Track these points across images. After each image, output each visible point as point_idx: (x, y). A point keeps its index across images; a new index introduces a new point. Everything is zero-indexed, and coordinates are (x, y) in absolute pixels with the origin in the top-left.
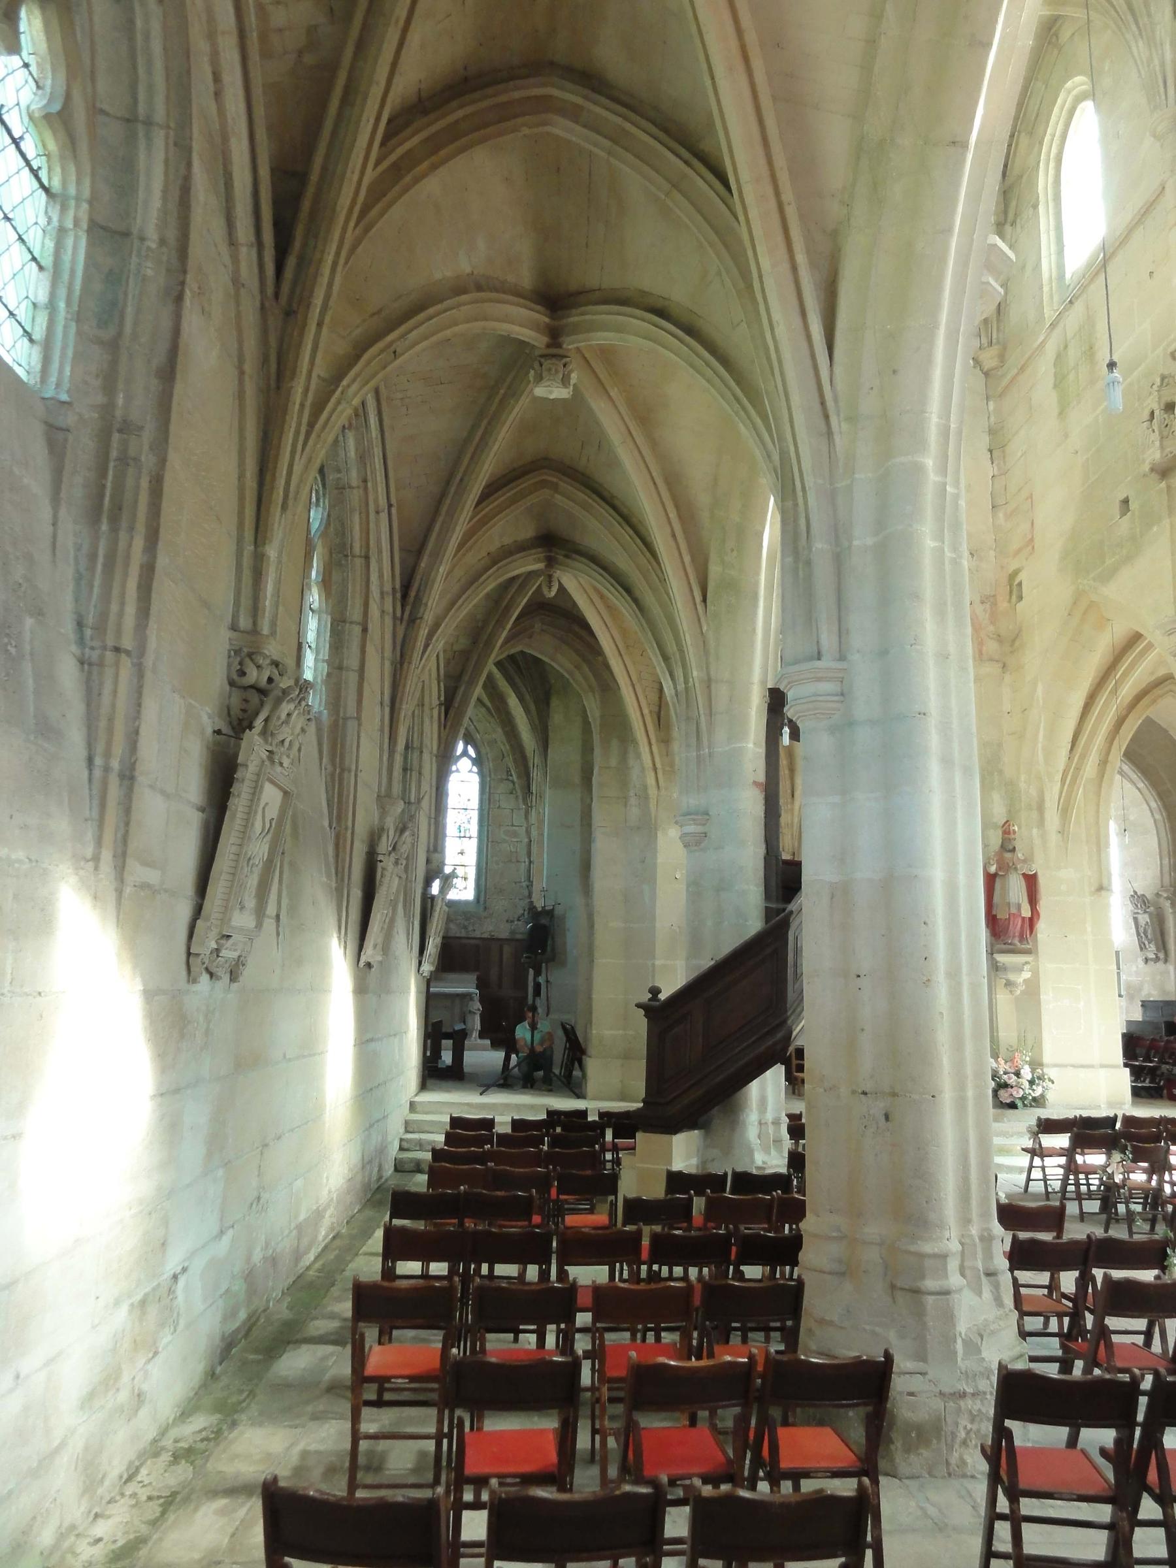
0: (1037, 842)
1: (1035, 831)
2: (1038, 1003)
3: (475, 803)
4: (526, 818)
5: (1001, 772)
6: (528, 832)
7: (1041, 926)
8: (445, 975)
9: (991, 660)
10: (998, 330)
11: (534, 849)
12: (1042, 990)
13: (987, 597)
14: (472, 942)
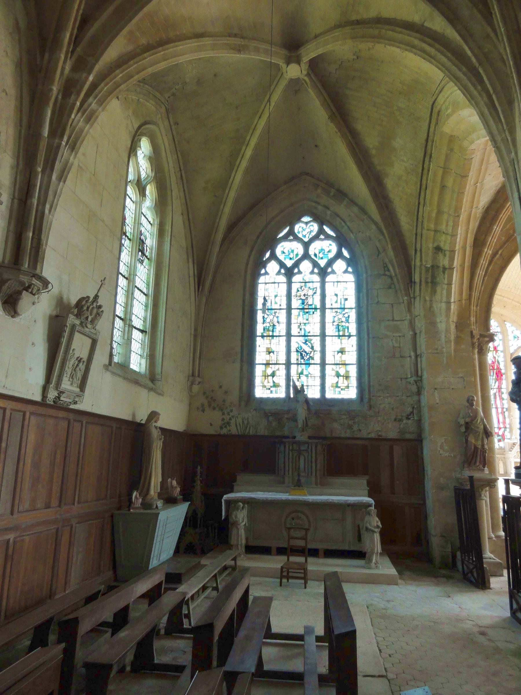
3: (352, 302)
4: (409, 310)
6: (412, 325)
11: (422, 341)
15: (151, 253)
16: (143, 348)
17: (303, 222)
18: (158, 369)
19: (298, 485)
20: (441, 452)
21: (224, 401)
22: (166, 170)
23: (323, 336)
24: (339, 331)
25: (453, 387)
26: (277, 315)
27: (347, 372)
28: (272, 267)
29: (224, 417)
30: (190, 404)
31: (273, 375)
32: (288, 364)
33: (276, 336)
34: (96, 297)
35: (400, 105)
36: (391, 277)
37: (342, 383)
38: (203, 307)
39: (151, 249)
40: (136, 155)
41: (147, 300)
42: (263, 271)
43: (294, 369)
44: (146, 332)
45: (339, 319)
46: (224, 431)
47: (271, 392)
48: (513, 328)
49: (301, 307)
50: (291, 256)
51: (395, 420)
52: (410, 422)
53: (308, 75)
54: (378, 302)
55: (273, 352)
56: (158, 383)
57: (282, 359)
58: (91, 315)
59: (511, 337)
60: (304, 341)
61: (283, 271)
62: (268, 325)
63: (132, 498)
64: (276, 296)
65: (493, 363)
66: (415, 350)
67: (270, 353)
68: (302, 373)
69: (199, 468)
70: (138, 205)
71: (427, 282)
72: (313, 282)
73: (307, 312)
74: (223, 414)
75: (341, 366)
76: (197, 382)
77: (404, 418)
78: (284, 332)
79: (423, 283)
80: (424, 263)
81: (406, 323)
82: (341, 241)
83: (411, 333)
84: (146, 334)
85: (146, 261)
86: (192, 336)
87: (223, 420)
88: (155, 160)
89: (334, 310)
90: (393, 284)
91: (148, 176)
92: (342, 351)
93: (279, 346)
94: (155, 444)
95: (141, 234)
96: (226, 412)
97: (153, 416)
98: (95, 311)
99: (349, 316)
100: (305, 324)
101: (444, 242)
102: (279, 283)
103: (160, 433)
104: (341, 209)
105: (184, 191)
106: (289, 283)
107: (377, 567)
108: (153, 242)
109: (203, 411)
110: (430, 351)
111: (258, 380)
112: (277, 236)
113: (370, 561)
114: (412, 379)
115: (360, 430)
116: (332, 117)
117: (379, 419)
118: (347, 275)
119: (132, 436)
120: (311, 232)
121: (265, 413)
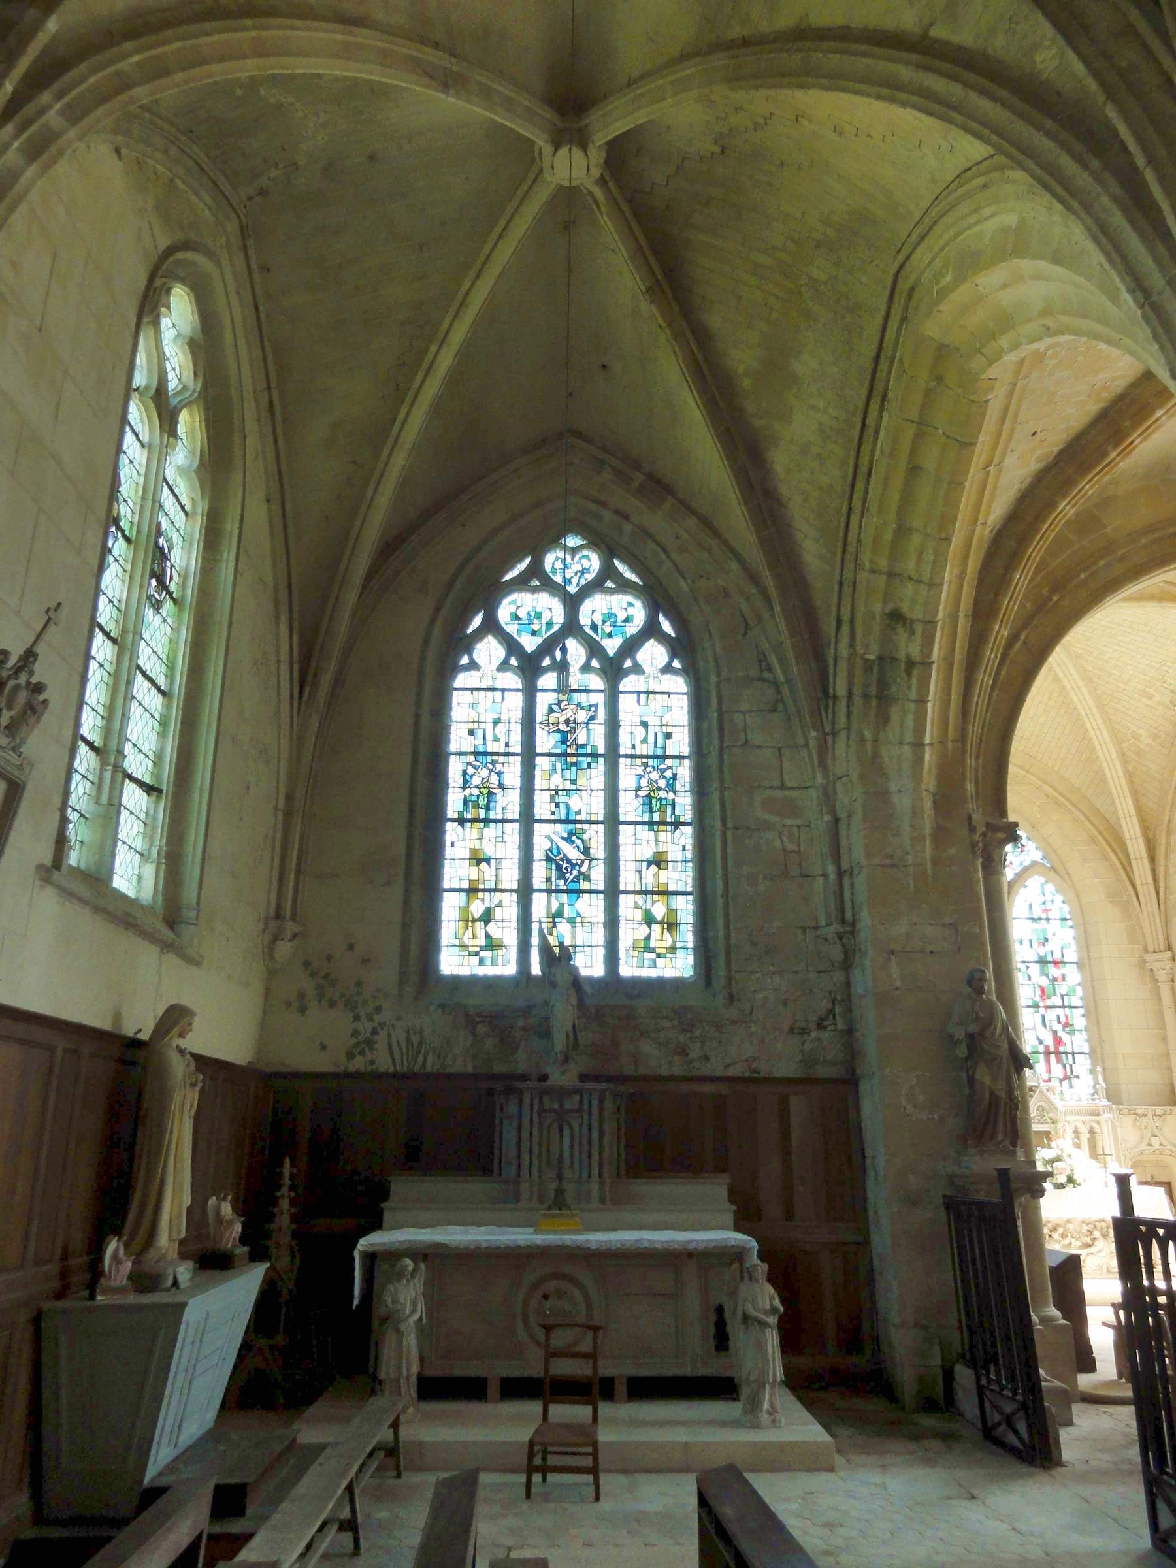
3: (681, 743)
4: (823, 764)
6: (828, 798)
8: (642, 1187)
14: (707, 1088)
15: (183, 586)
16: (148, 834)
17: (565, 548)
18: (190, 893)
19: (559, 1202)
20: (910, 1109)
21: (359, 984)
22: (233, 380)
23: (612, 822)
24: (651, 811)
25: (930, 948)
26: (499, 767)
27: (671, 911)
28: (489, 651)
29: (357, 1025)
30: (267, 993)
31: (487, 917)
32: (525, 892)
33: (496, 821)
34: (29, 656)
35: (815, 273)
36: (776, 685)
37: (660, 938)
38: (310, 741)
39: (184, 577)
40: (156, 323)
41: (168, 706)
42: (465, 660)
43: (539, 903)
44: (160, 791)
45: (651, 782)
46: (358, 1064)
47: (482, 962)
49: (559, 751)
50: (536, 627)
51: (792, 1030)
52: (826, 1035)
53: (602, 182)
54: (746, 742)
55: (488, 861)
56: (187, 931)
57: (511, 877)
58: (10, 707)
60: (565, 835)
61: (514, 661)
62: (476, 792)
63: (101, 1259)
64: (496, 722)
66: (836, 856)
67: (478, 862)
68: (559, 914)
69: (287, 1162)
70: (158, 453)
71: (866, 696)
72: (587, 691)
73: (574, 764)
74: (357, 1018)
75: (656, 897)
76: (289, 934)
77: (813, 1026)
78: (514, 812)
79: (858, 700)
80: (860, 650)
81: (813, 793)
82: (657, 597)
83: (827, 818)
84: (159, 798)
85: (169, 603)
86: (280, 816)
87: (356, 1033)
88: (205, 346)
89: (639, 761)
90: (782, 701)
91: (185, 388)
92: (659, 861)
93: (503, 844)
94: (177, 1098)
95: (159, 533)
96: (363, 1014)
97: (175, 1018)
98: (23, 696)
99: (675, 777)
100: (568, 792)
101: (909, 599)
102: (503, 690)
103: (193, 1067)
104: (657, 521)
105: (276, 441)
106: (530, 693)
107: (774, 1421)
108: (189, 559)
109: (303, 1010)
110: (877, 861)
111: (448, 931)
112: (503, 577)
113: (754, 1404)
114: (831, 930)
115: (707, 1058)
116: (654, 291)
117: (753, 1029)
118: (668, 677)
119: (116, 1077)
120: (584, 571)
121: (467, 1015)
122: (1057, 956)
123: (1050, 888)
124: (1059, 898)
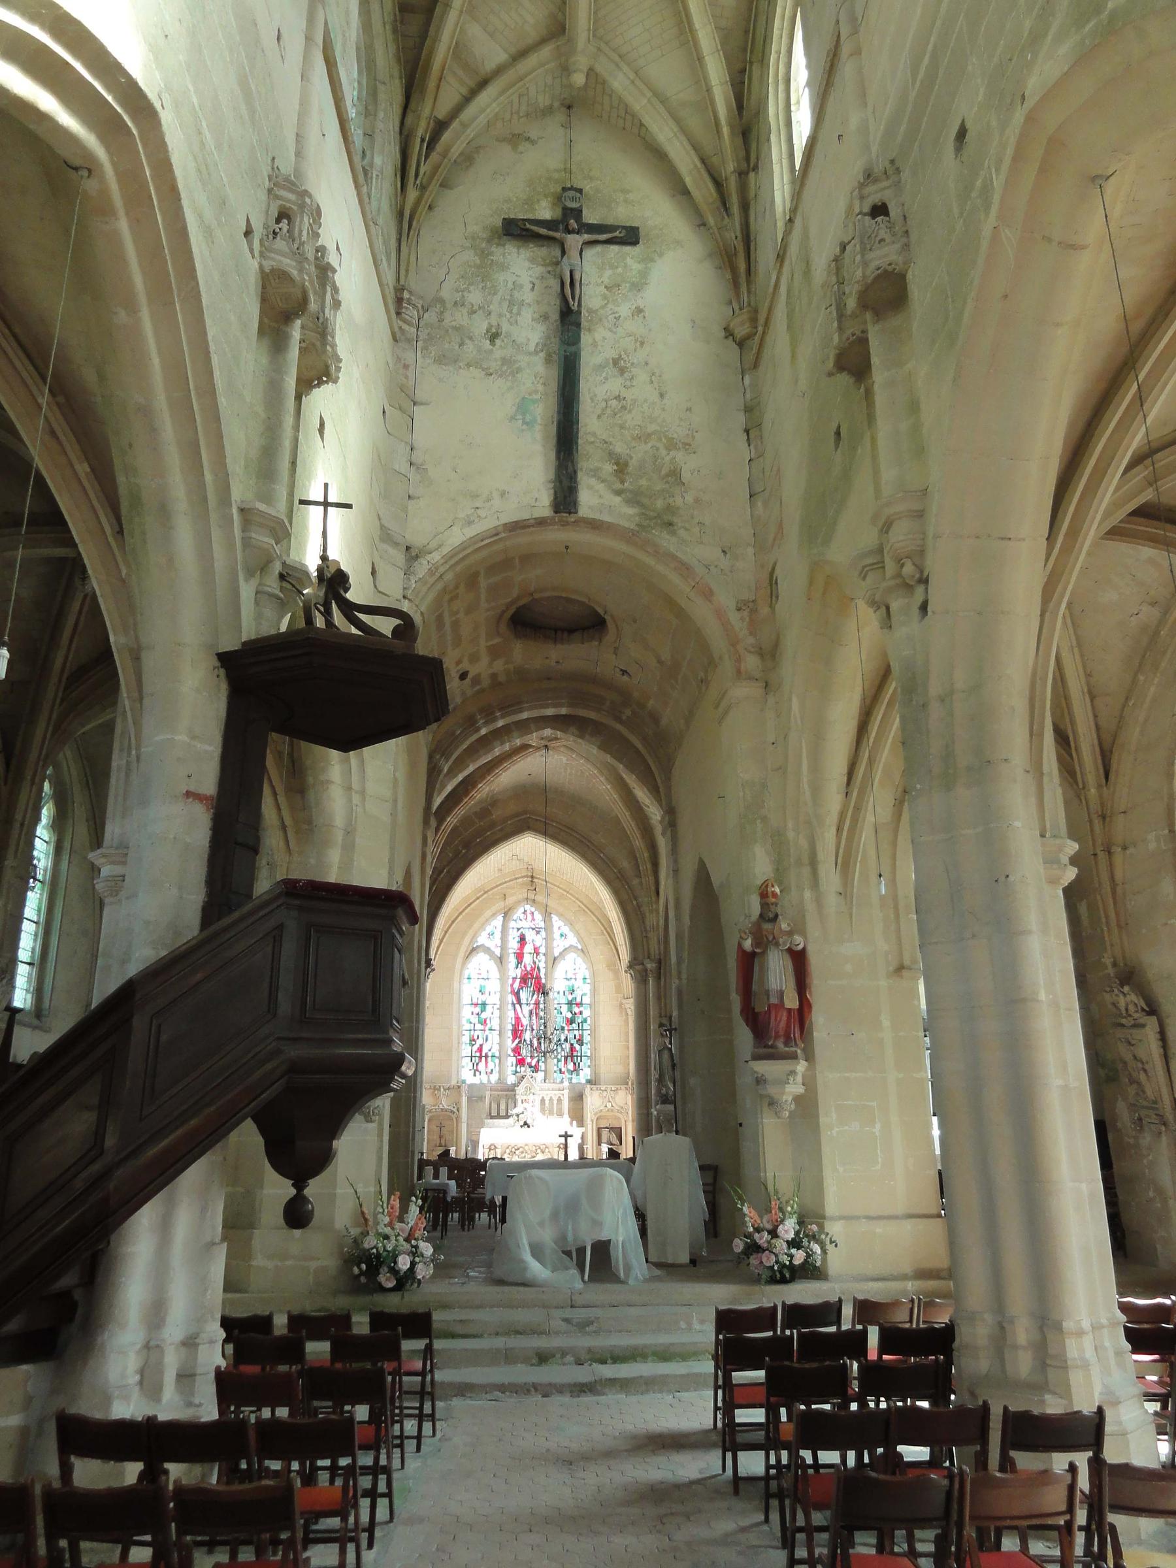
0: (810, 907)
1: (808, 894)
2: (816, 1129)
5: (764, 819)
7: (819, 1019)
9: (750, 678)
10: (749, 292)
12: (821, 1112)
13: (746, 603)
15: (45, 875)
16: (29, 981)
18: (46, 1004)
39: (45, 870)
41: (37, 928)
48: (561, 923)
56: (44, 1019)
59: (556, 935)
65: (533, 969)
122: (579, 1000)
123: (579, 960)
124: (584, 966)
